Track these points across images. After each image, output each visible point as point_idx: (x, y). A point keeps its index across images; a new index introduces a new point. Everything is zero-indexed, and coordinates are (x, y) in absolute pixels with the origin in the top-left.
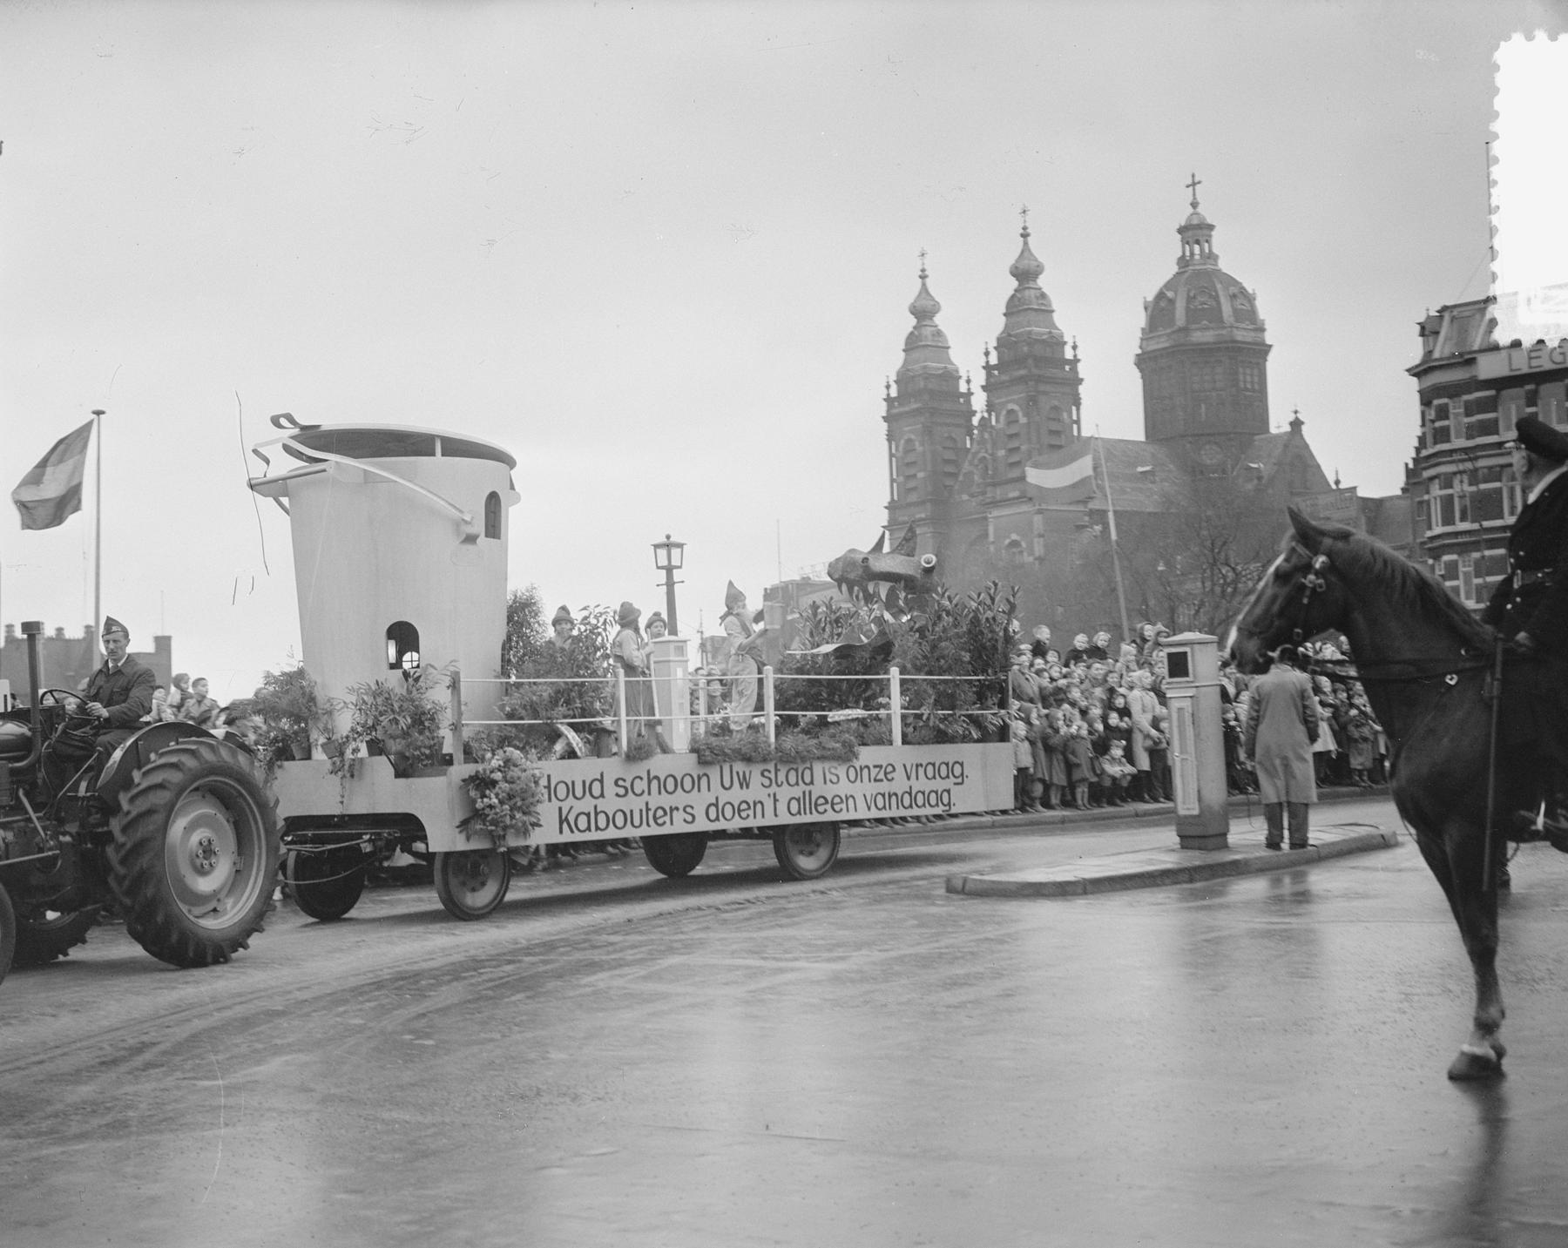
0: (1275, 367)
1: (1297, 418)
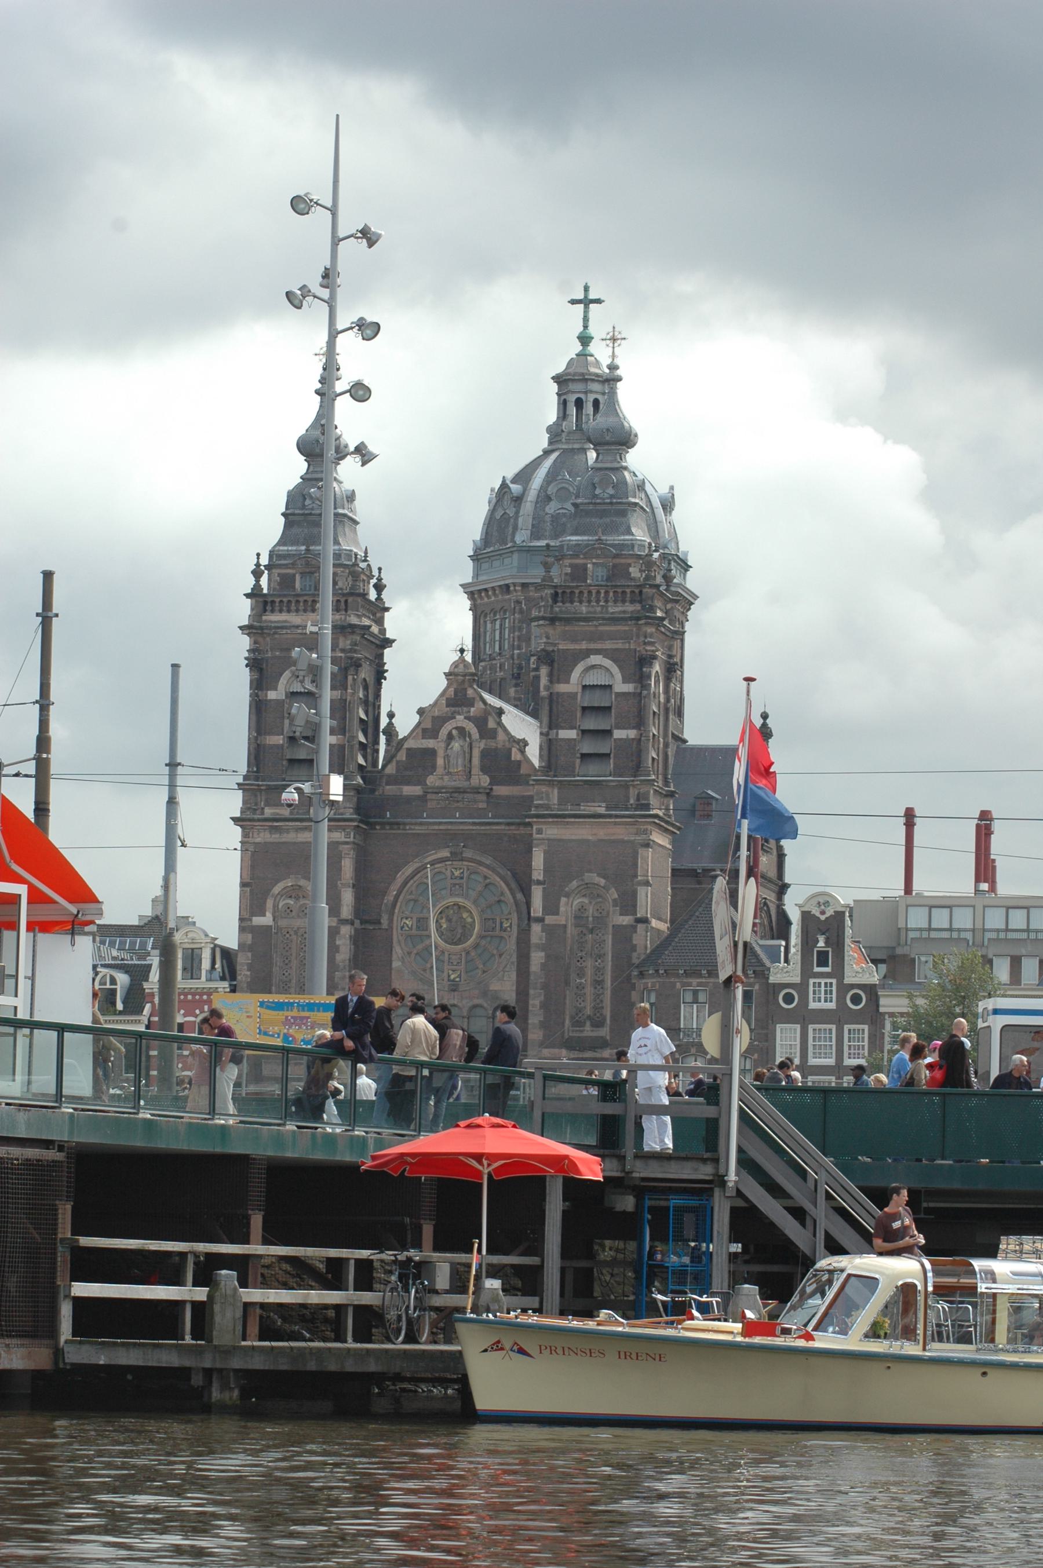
1: (764, 725)
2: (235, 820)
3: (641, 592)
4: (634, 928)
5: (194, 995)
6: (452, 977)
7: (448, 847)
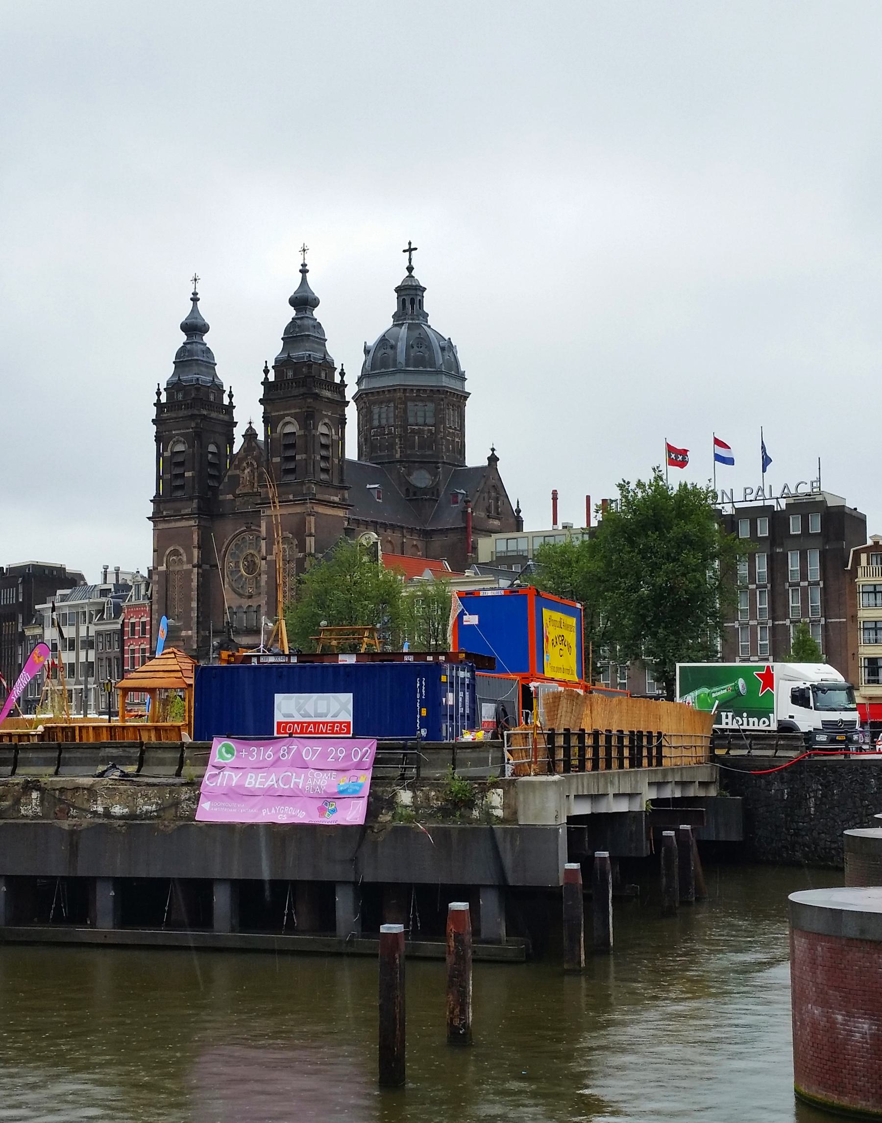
0: (471, 408)
1: (493, 454)
2: (149, 518)
4: (304, 559)
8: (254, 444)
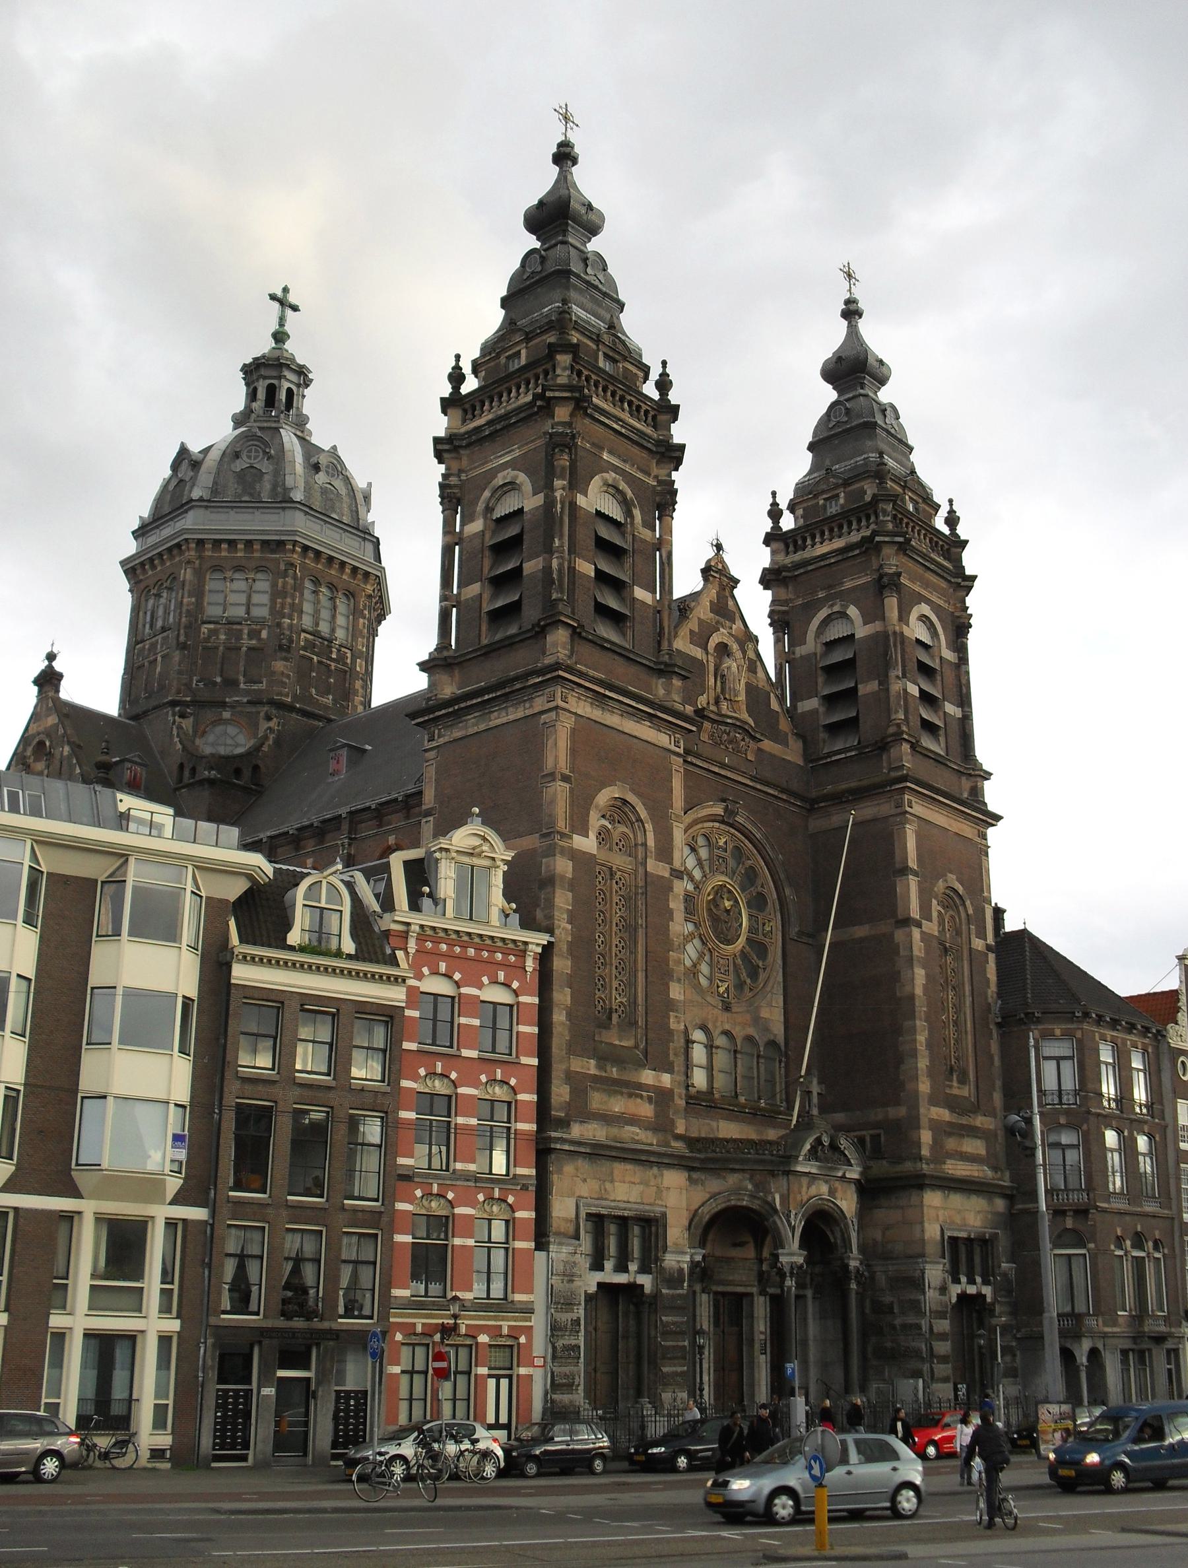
3: (948, 550)
5: (479, 949)
6: (721, 990)
7: (724, 800)
8: (731, 603)
